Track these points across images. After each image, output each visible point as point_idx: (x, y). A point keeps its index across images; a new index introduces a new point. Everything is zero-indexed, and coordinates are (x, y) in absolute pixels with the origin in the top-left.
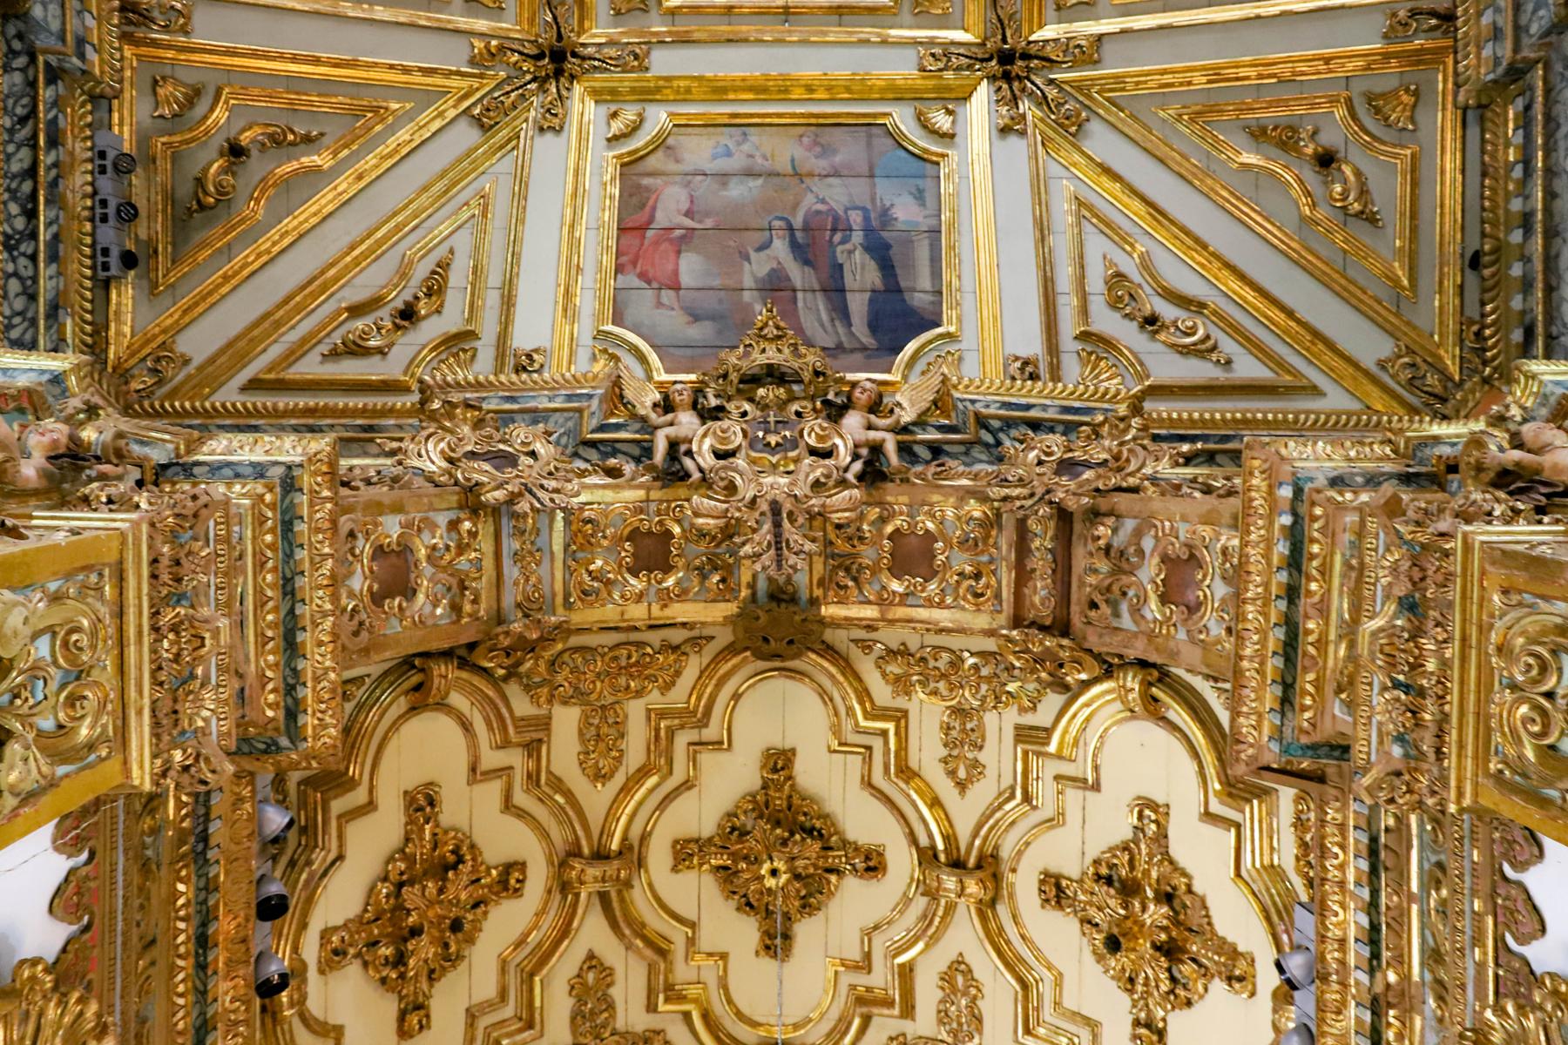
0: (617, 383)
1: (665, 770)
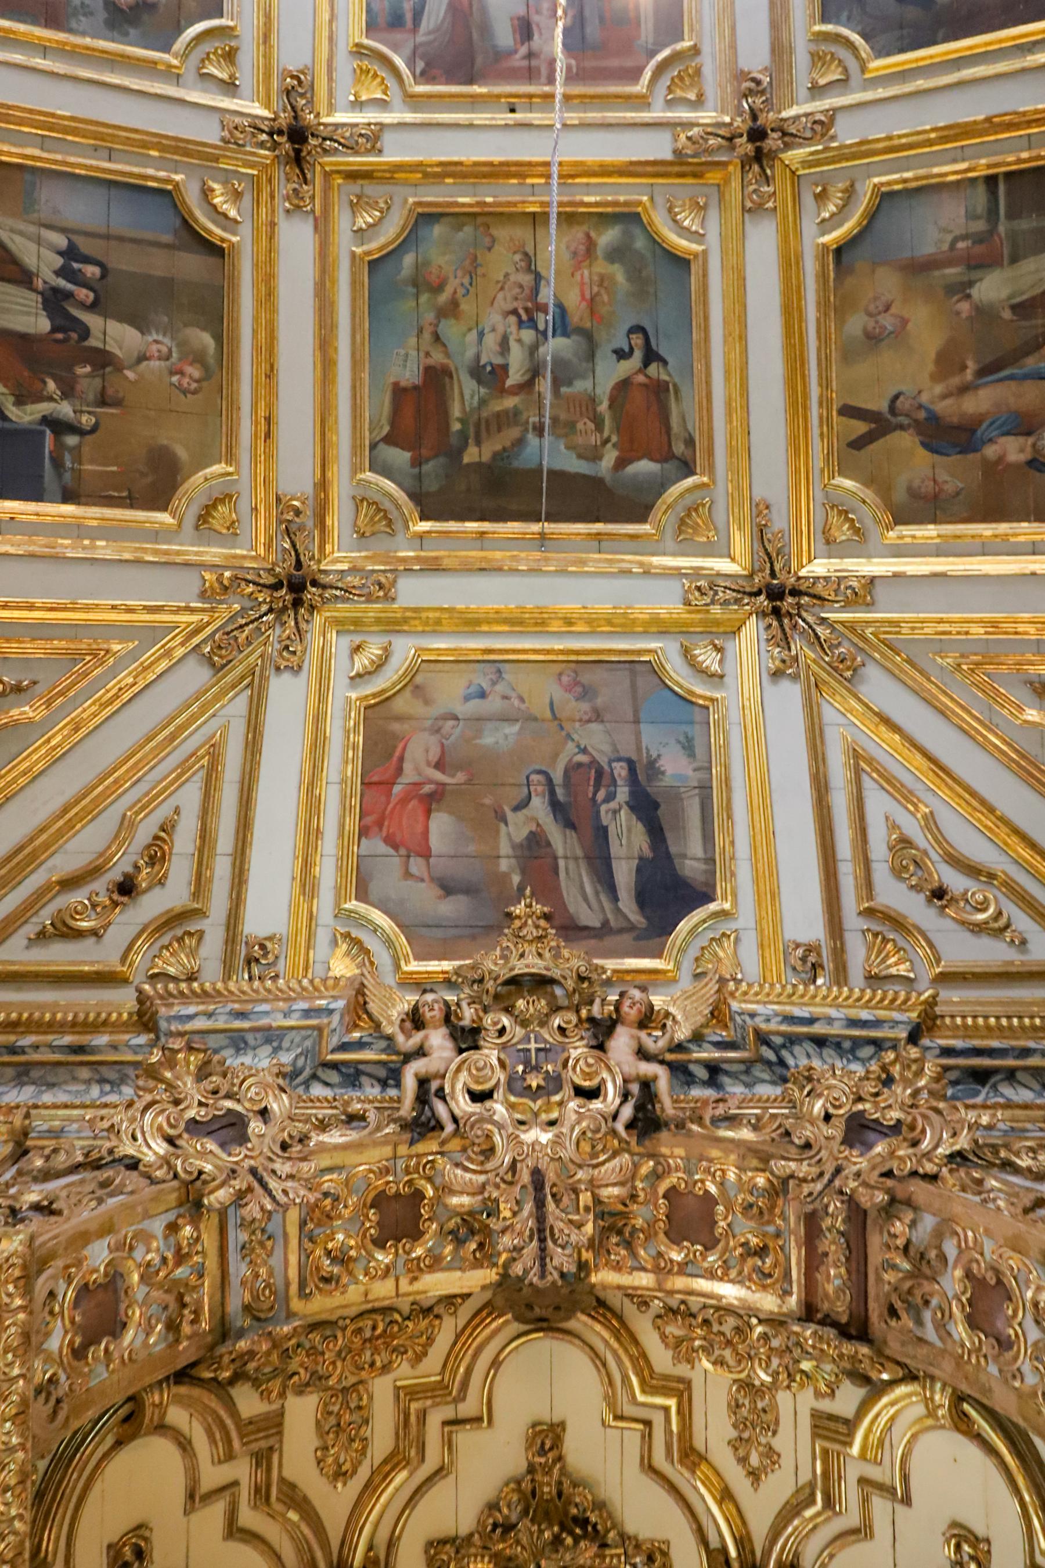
0: (361, 991)
1: (415, 1462)
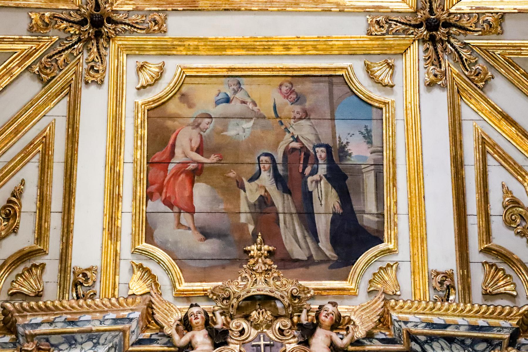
0: (150, 306)
